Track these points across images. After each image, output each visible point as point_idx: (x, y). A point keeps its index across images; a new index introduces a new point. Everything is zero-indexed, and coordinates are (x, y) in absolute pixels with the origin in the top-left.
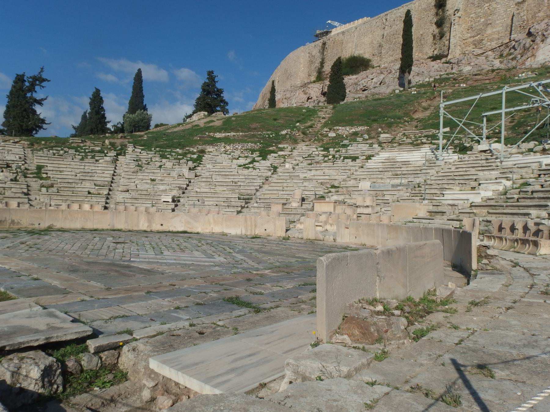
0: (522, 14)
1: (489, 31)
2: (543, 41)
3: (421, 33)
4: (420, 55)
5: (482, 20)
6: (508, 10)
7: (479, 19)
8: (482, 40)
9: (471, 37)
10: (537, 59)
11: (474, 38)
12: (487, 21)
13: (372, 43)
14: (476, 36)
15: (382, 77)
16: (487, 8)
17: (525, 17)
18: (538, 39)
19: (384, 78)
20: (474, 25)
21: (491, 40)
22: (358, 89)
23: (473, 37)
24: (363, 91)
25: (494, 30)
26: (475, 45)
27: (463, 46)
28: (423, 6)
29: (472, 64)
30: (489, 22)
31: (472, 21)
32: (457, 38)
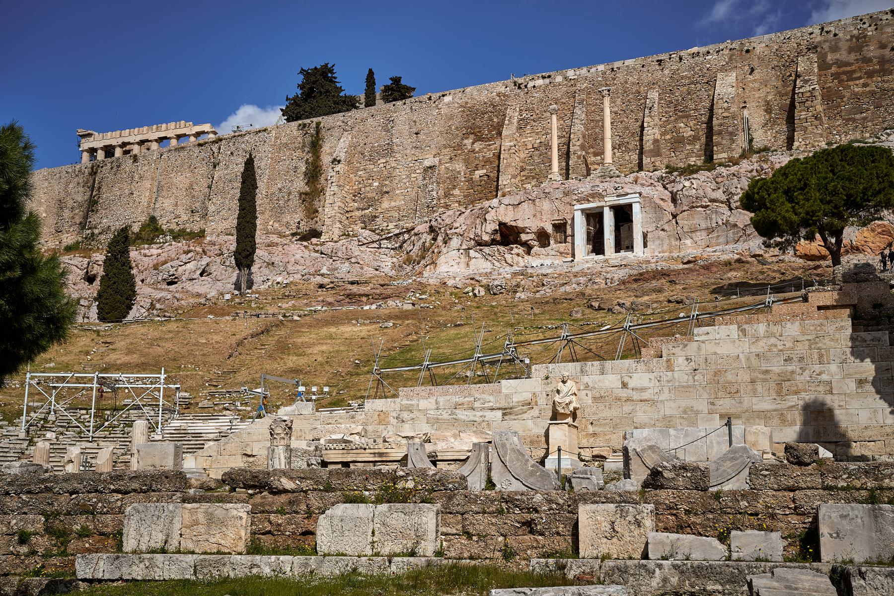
0: (430, 187)
1: (386, 205)
2: (445, 243)
3: (279, 186)
4: (276, 225)
5: (376, 184)
6: (413, 175)
7: (370, 181)
8: (375, 217)
9: (358, 209)
10: (438, 270)
11: (364, 212)
12: (382, 186)
13: (191, 187)
14: (365, 209)
15: (205, 260)
16: (382, 165)
17: (434, 193)
18: (440, 238)
19: (208, 265)
20: (363, 189)
21: (389, 220)
22: (160, 278)
23: (363, 209)
24: (170, 284)
25: (393, 204)
26: (364, 222)
27: (346, 222)
28: (284, 140)
29: (353, 260)
30: (385, 190)
31: (360, 183)
32: (336, 208)
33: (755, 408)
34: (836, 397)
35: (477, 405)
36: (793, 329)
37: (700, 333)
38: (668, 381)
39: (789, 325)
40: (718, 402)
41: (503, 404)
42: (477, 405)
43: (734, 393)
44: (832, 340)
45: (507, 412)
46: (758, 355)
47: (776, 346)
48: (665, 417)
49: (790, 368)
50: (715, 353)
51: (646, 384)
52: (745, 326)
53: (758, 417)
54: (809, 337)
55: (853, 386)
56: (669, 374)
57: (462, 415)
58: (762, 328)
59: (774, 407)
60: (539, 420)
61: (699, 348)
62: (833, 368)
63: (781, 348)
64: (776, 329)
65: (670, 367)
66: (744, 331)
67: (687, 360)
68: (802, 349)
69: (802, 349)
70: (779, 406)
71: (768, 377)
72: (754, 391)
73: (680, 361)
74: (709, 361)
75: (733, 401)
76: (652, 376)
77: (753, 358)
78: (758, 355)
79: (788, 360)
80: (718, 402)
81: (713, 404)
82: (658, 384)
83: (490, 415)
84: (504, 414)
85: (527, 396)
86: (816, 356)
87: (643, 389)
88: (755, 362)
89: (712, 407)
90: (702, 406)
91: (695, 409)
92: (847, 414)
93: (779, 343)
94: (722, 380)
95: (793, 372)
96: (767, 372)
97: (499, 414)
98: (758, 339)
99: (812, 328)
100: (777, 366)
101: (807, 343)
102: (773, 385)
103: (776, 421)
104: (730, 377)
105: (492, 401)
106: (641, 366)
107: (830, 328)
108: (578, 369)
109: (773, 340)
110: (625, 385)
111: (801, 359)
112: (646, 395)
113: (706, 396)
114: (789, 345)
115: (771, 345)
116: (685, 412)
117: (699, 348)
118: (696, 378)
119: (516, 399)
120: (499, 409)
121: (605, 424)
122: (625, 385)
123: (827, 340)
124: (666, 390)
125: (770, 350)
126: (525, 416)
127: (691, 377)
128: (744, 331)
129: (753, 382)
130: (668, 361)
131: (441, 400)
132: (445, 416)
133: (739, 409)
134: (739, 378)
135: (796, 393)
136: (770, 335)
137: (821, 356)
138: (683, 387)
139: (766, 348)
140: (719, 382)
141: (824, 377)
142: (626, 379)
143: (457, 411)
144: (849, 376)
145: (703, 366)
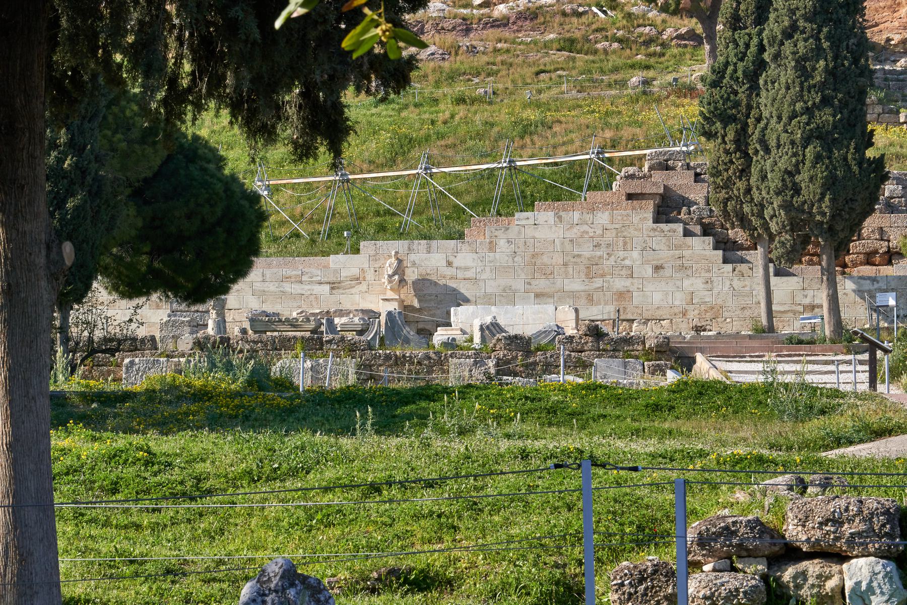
33: (566, 288)
34: (635, 281)
35: (305, 278)
36: (603, 218)
37: (521, 217)
38: (490, 262)
39: (600, 214)
40: (533, 282)
41: (332, 279)
42: (305, 278)
43: (548, 274)
44: (636, 230)
45: (334, 286)
46: (572, 241)
47: (587, 233)
48: (486, 295)
49: (598, 253)
50: (534, 238)
51: (470, 263)
52: (561, 213)
53: (569, 297)
54: (617, 226)
55: (649, 270)
56: (491, 254)
57: (287, 287)
58: (577, 215)
59: (583, 288)
60: (367, 294)
61: (519, 232)
62: (635, 254)
63: (591, 234)
64: (588, 217)
65: (492, 247)
66: (560, 218)
67: (508, 242)
68: (609, 236)
69: (609, 236)
70: (587, 288)
71: (579, 260)
72: (566, 273)
73: (502, 243)
74: (528, 244)
75: (547, 282)
76: (475, 256)
77: (567, 242)
78: (572, 241)
79: (597, 246)
80: (533, 282)
81: (529, 284)
82: (480, 264)
83: (318, 289)
84: (332, 288)
85: (355, 271)
86: (621, 244)
87: (467, 269)
88: (568, 247)
89: (529, 287)
90: (519, 285)
91: (513, 288)
92: (644, 296)
93: (590, 230)
94: (538, 262)
95: (600, 257)
96: (579, 256)
97: (327, 288)
98: (572, 225)
99: (619, 218)
100: (587, 251)
101: (614, 232)
102: (582, 268)
103: (583, 301)
104: (545, 259)
105: (319, 275)
106: (465, 247)
107: (636, 219)
108: (406, 246)
109: (585, 228)
110: (449, 264)
111: (608, 245)
112: (469, 274)
113: (523, 276)
114: (599, 232)
115: (583, 232)
116: (504, 291)
117: (519, 232)
118: (516, 259)
119: (344, 274)
120: (327, 283)
121: (431, 300)
122: (449, 264)
123: (631, 230)
124: (488, 269)
125: (582, 237)
126: (353, 291)
127: (511, 259)
128: (560, 218)
129: (565, 265)
130: (491, 242)
131: (268, 273)
132: (272, 287)
133: (553, 290)
134: (554, 260)
135: (602, 276)
136: (583, 222)
137: (625, 244)
138: (504, 267)
139: (579, 234)
140: (536, 266)
141: (627, 262)
142: (451, 259)
143: (284, 284)
144: (647, 262)
145: (522, 248)
